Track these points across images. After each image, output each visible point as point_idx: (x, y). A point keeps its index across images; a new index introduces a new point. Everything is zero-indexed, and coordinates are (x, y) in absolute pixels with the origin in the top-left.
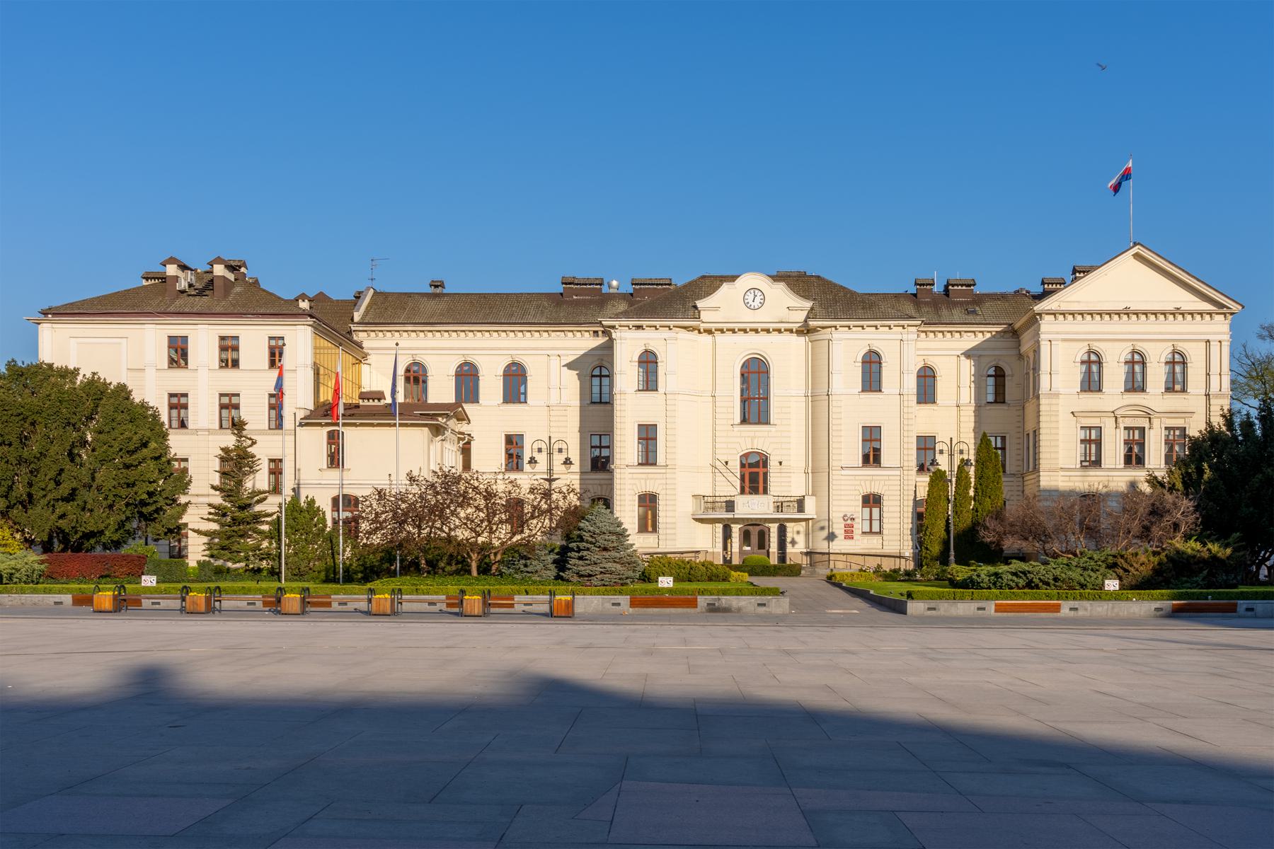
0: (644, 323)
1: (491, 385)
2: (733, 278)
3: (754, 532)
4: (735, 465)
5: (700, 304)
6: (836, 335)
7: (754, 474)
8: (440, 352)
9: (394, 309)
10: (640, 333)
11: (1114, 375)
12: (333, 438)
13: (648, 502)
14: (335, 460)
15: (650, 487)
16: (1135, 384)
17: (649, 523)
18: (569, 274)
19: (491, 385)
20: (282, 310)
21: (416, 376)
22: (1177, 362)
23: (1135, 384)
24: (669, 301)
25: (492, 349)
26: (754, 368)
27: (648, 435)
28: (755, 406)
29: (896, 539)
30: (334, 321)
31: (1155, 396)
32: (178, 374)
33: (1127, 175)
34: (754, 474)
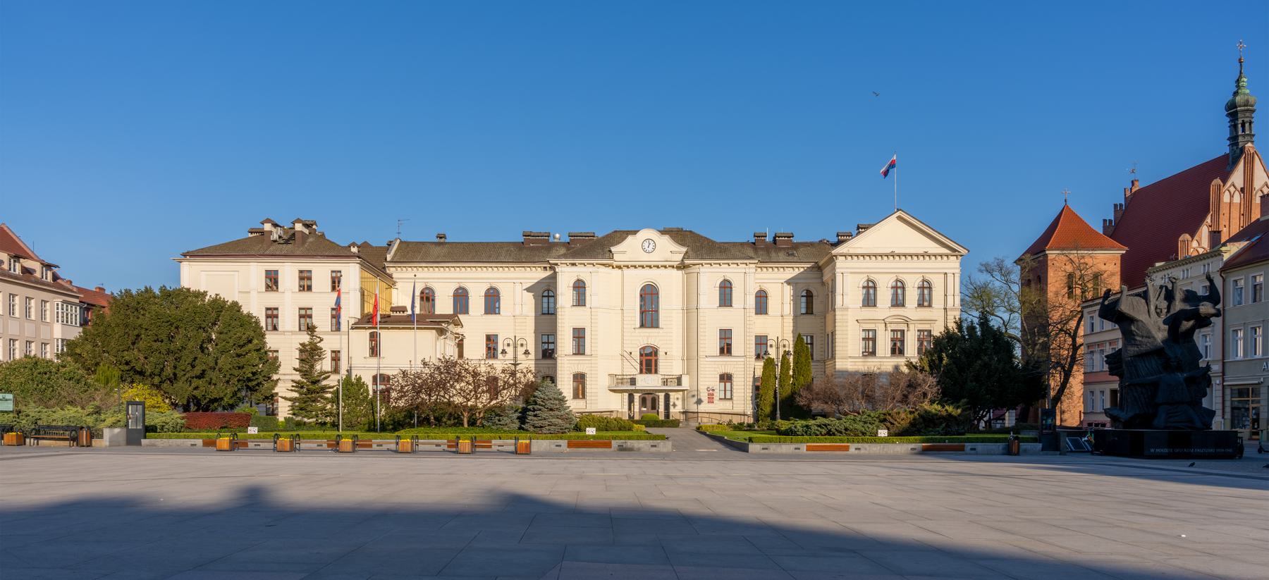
0: (577, 262)
1: (477, 302)
2: (635, 232)
3: (649, 398)
4: (637, 355)
5: (613, 249)
6: (702, 269)
7: (649, 361)
8: (444, 281)
9: (413, 253)
10: (574, 268)
11: (884, 296)
12: (373, 337)
13: (580, 379)
14: (374, 351)
15: (581, 370)
16: (898, 302)
17: (580, 393)
18: (528, 229)
19: (477, 302)
20: (340, 253)
21: (428, 297)
22: (926, 288)
23: (898, 302)
24: (593, 247)
25: (477, 279)
26: (649, 291)
27: (579, 335)
28: (649, 317)
29: (742, 403)
30: (374, 261)
31: (911, 309)
32: (271, 295)
33: (892, 165)
34: (649, 361)
